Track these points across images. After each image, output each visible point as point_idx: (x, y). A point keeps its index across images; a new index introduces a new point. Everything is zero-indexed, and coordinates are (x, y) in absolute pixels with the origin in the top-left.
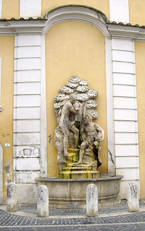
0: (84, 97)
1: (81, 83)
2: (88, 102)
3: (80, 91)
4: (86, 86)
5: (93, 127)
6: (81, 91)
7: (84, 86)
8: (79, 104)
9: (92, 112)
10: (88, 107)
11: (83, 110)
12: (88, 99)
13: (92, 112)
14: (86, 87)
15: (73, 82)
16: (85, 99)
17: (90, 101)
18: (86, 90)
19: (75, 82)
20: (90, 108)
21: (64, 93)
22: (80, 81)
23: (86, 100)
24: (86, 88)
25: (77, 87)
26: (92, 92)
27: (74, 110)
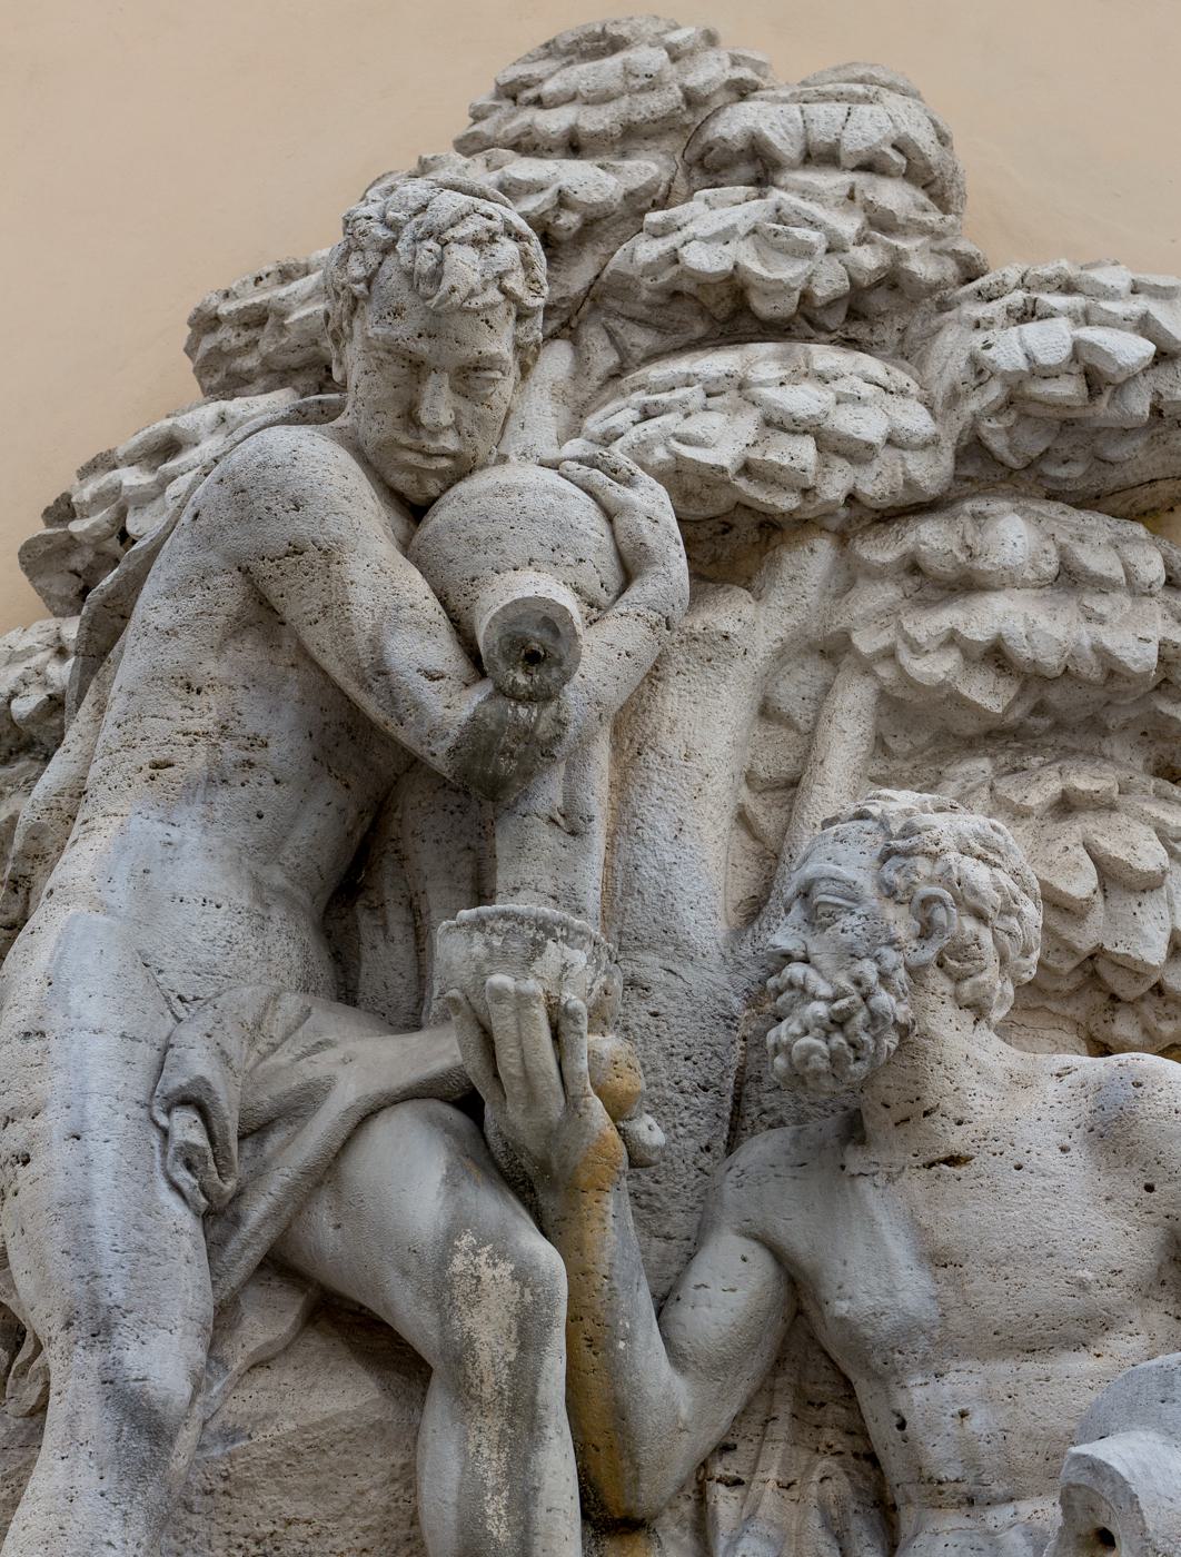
0: (802, 400)
1: (734, 123)
2: (931, 537)
3: (705, 259)
4: (870, 166)
5: (1076, 1173)
6: (735, 287)
7: (832, 182)
8: (617, 493)
9: (1066, 806)
10: (936, 668)
11: (793, 784)
12: (930, 472)
13: (1066, 806)
14: (894, 196)
15: (554, 122)
16: (858, 453)
17: (1014, 535)
18: (869, 259)
19: (595, 120)
20: (989, 695)
21: (278, 375)
22: (742, 91)
23: (876, 483)
24: (881, 223)
25: (638, 205)
26: (1068, 288)
27: (441, 652)
